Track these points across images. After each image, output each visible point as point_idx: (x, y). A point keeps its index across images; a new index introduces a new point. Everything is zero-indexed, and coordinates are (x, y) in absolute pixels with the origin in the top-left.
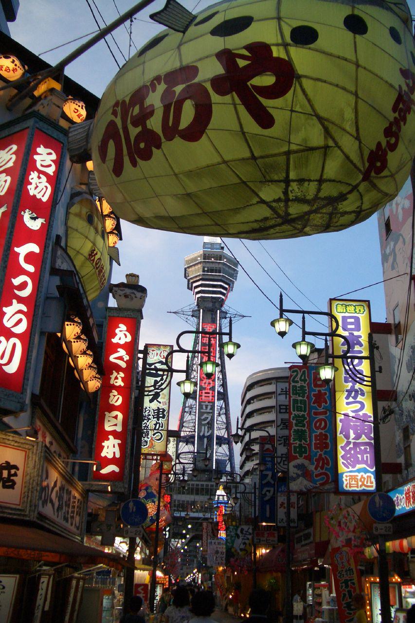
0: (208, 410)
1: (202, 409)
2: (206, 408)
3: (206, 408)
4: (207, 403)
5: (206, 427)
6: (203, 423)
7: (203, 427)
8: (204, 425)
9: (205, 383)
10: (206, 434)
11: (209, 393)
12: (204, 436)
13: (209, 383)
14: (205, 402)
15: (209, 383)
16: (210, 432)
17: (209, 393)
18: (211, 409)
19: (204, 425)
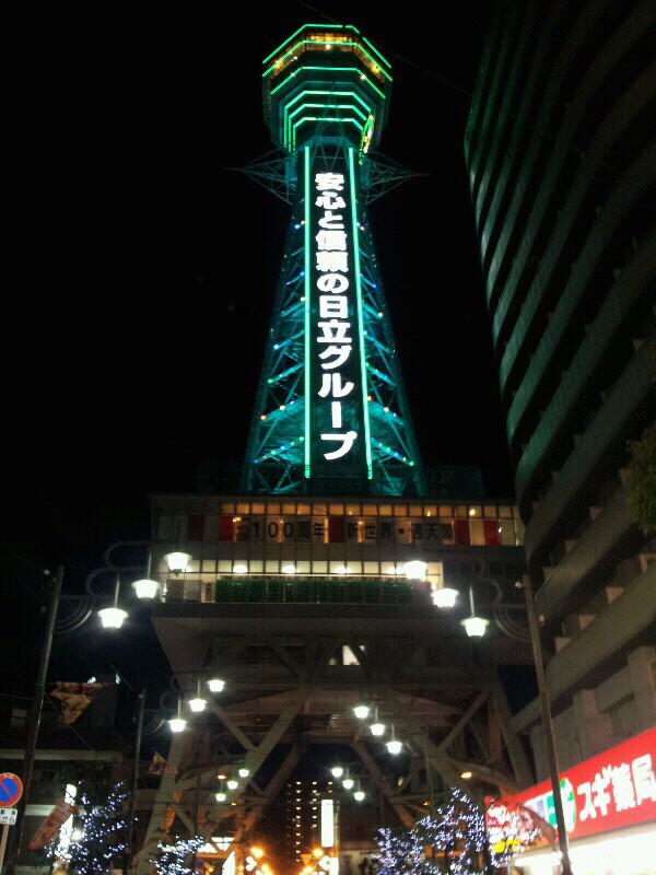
0: (340, 338)
1: (322, 334)
2: (334, 331)
3: (334, 331)
4: (334, 324)
5: (337, 377)
6: (325, 366)
7: (326, 378)
8: (331, 372)
9: (326, 284)
10: (338, 393)
11: (338, 302)
12: (330, 398)
13: (338, 283)
14: (328, 320)
15: (338, 283)
16: (350, 386)
17: (338, 302)
18: (347, 335)
19: (331, 372)
